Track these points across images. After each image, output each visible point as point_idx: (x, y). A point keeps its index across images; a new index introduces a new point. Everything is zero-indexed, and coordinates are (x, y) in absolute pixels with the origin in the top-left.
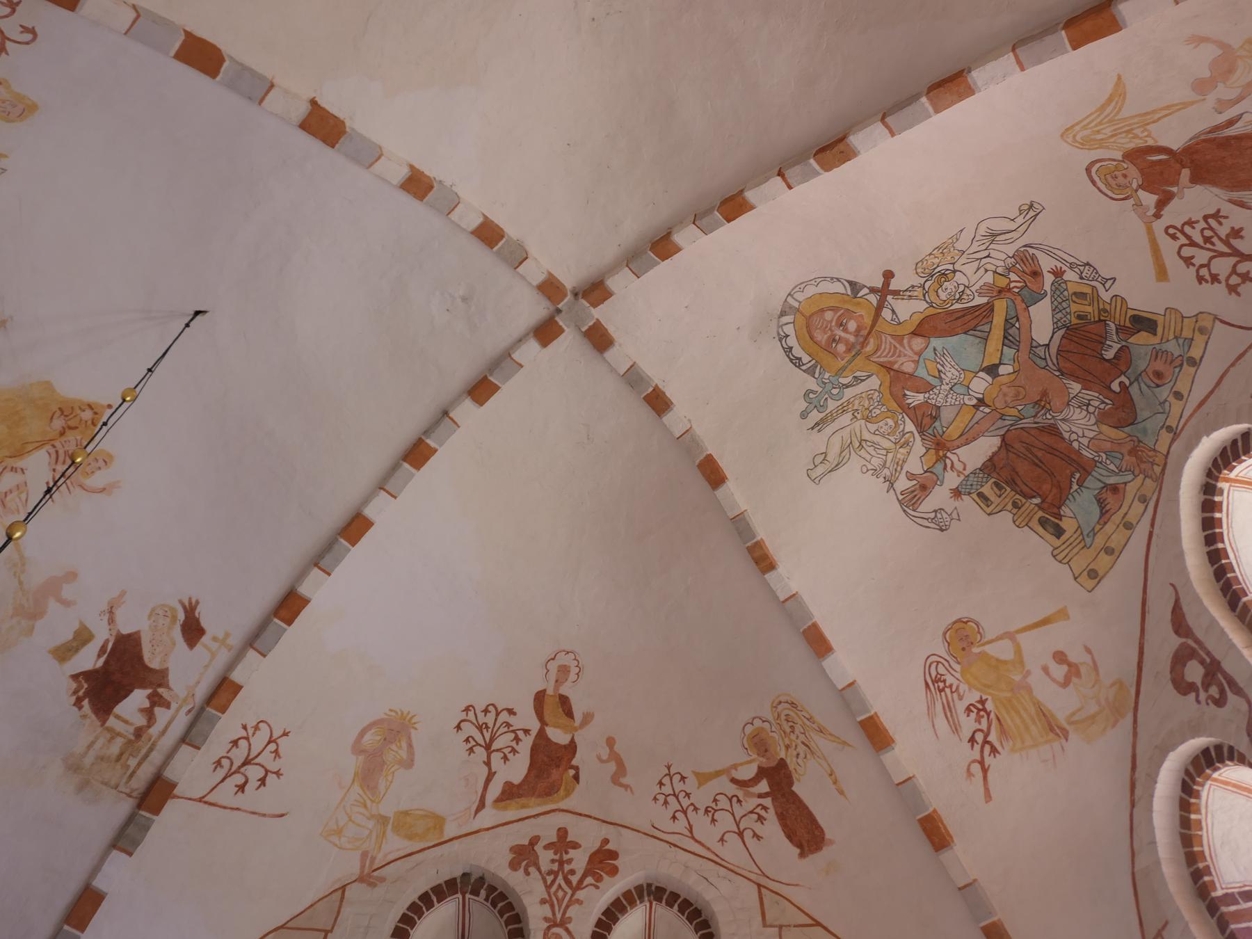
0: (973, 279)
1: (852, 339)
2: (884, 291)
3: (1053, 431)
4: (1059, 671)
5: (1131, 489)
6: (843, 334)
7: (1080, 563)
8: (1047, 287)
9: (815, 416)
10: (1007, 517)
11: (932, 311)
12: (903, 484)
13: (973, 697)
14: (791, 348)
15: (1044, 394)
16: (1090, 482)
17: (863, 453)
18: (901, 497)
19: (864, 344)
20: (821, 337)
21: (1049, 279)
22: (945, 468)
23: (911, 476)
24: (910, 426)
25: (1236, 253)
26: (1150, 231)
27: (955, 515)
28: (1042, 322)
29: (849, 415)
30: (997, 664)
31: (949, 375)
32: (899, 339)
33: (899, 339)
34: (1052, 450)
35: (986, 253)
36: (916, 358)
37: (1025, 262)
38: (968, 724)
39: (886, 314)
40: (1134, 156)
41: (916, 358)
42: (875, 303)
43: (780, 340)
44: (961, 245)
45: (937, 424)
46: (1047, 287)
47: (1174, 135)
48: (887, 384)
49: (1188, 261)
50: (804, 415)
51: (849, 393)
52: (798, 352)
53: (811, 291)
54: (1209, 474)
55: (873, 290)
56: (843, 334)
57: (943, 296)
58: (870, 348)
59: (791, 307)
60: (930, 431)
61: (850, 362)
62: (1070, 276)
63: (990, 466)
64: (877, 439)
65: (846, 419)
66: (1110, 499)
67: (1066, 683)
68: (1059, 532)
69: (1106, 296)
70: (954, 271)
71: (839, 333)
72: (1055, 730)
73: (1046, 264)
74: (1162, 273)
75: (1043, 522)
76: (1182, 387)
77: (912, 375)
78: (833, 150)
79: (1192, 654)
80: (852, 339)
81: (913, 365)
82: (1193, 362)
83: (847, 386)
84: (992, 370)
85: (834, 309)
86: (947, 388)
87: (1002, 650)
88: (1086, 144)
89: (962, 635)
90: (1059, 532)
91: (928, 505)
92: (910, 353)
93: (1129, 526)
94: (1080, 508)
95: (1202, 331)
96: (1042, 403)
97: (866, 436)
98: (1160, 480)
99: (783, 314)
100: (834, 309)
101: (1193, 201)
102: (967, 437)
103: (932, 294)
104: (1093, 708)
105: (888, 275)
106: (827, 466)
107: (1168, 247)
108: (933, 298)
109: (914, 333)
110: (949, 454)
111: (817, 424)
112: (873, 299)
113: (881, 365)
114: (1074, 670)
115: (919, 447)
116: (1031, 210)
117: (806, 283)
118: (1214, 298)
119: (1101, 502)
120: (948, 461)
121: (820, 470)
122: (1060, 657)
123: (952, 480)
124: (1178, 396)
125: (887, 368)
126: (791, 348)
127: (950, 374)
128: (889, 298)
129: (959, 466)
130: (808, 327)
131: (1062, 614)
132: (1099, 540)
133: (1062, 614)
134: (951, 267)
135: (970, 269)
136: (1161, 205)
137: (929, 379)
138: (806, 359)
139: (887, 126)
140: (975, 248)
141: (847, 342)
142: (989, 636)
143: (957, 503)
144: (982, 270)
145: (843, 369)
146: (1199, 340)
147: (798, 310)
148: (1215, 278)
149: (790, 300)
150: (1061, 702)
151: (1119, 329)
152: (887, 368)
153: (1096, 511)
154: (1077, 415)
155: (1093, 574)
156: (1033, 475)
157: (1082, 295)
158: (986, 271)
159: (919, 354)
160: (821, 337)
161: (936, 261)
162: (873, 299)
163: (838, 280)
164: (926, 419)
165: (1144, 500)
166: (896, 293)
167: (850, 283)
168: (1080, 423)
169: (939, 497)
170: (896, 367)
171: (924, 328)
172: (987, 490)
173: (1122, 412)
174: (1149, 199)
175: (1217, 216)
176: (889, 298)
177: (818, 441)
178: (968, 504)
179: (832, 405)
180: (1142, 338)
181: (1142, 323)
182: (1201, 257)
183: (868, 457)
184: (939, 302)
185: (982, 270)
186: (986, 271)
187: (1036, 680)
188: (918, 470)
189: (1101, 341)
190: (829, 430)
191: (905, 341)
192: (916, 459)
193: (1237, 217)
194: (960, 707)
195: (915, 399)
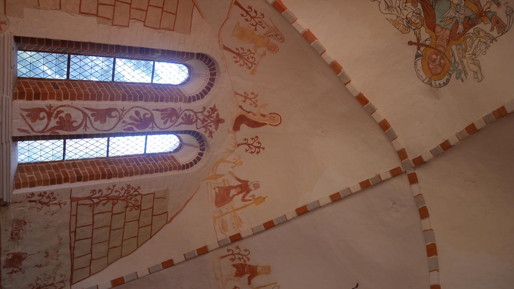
0: (410, 10)
1: (439, 57)
2: (419, 45)
6: (438, 61)
9: (463, 75)
11: (425, 25)
12: (495, 33)
14: (444, 83)
17: (477, 54)
18: (500, 34)
19: (441, 52)
20: (439, 70)
22: (489, 12)
23: (492, 30)
24: (471, 31)
27: (506, 5)
29: (464, 59)
31: (452, 14)
32: (437, 37)
33: (437, 37)
35: (398, 9)
36: (444, 29)
39: (428, 43)
41: (444, 29)
42: (424, 48)
43: (441, 87)
44: (394, 18)
45: (472, 17)
48: (454, 41)
50: (463, 81)
51: (457, 59)
52: (444, 80)
53: (421, 73)
55: (419, 49)
56: (438, 61)
57: (418, 21)
58: (442, 50)
59: (429, 81)
60: (474, 20)
61: (447, 58)
64: (474, 46)
65: (465, 61)
70: (407, 18)
71: (437, 62)
77: (451, 31)
78: (335, 67)
80: (439, 57)
81: (447, 31)
83: (455, 60)
85: (428, 64)
86: (457, 14)
91: (504, 19)
92: (442, 33)
97: (471, 52)
99: (431, 85)
100: (428, 64)
103: (417, 25)
105: (410, 43)
106: (478, 72)
108: (419, 25)
109: (434, 31)
110: (484, 10)
111: (465, 74)
112: (422, 48)
113: (448, 44)
117: (418, 76)
120: (487, 10)
121: (479, 76)
123: (494, 8)
125: (448, 42)
126: (444, 83)
127: (451, 13)
128: (421, 42)
129: (488, 6)
130: (436, 75)
134: (405, 20)
135: (405, 13)
137: (453, 23)
138: (446, 77)
139: (322, 54)
140: (396, 13)
141: (440, 59)
143: (502, 4)
144: (406, 8)
145: (449, 61)
147: (430, 79)
149: (425, 81)
158: (406, 6)
159: (442, 28)
160: (439, 70)
161: (401, 26)
162: (422, 48)
163: (415, 62)
164: (469, 23)
166: (418, 40)
167: (416, 57)
170: (448, 38)
171: (432, 27)
176: (421, 42)
177: (470, 74)
183: (480, 51)
184: (421, 23)
185: (406, 8)
186: (406, 6)
188: (490, 25)
190: (467, 70)
191: (438, 34)
192: (485, 27)
195: (461, 27)
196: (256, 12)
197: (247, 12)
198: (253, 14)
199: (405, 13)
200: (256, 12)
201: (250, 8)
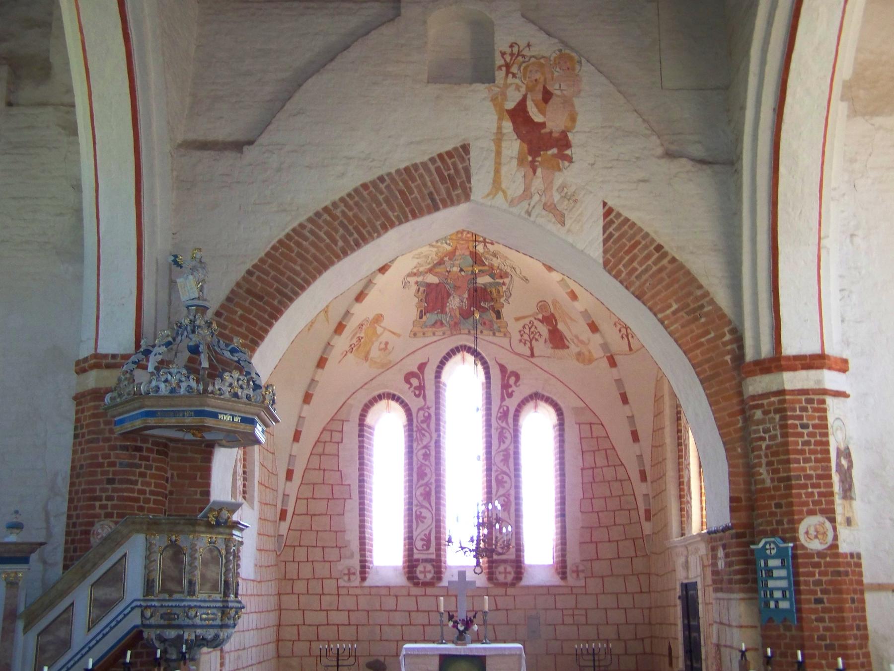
3: (449, 295)
4: (383, 346)
5: (444, 328)
7: (416, 329)
8: (498, 280)
10: (416, 300)
13: (362, 335)
15: (459, 287)
16: (440, 316)
21: (501, 281)
25: (531, 341)
26: (530, 316)
28: (483, 280)
30: (375, 333)
34: (443, 298)
37: (503, 275)
38: (354, 341)
40: (553, 316)
46: (498, 280)
47: (561, 326)
49: (524, 327)
51: (445, 245)
54: (461, 346)
62: (504, 288)
63: (429, 285)
66: (439, 324)
67: (380, 350)
68: (421, 318)
69: (502, 300)
72: (366, 358)
73: (507, 281)
74: (517, 319)
75: (421, 311)
76: (485, 332)
79: (419, 378)
82: (494, 334)
84: (461, 270)
87: (379, 330)
88: (553, 303)
89: (378, 319)
90: (421, 318)
93: (434, 334)
94: (430, 318)
95: (505, 335)
96: (456, 288)
98: (452, 335)
101: (544, 330)
102: (436, 274)
104: (378, 361)
107: (527, 321)
114: (386, 348)
115: (428, 267)
116: (526, 280)
118: (516, 336)
119: (436, 323)
122: (387, 344)
123: (420, 279)
124: (482, 332)
125: (456, 249)
127: (457, 262)
131: (399, 336)
132: (426, 329)
133: (399, 336)
136: (539, 320)
142: (383, 324)
146: (502, 334)
148: (522, 336)
150: (375, 353)
151: (493, 306)
152: (456, 249)
153: (433, 321)
154: (457, 300)
155: (415, 335)
156: (433, 299)
157: (499, 291)
164: (441, 263)
165: (444, 334)
168: (455, 303)
169: (413, 280)
172: (422, 289)
173: (466, 314)
174: (540, 316)
175: (540, 335)
178: (415, 287)
179: (439, 244)
180: (494, 315)
181: (498, 315)
182: (527, 331)
187: (376, 344)
189: (485, 301)
193: (542, 340)
194: (358, 335)
195: (446, 259)
196: (620, 331)
197: (627, 336)
198: (624, 331)
199: (499, 261)
200: (620, 331)
201: (622, 337)
